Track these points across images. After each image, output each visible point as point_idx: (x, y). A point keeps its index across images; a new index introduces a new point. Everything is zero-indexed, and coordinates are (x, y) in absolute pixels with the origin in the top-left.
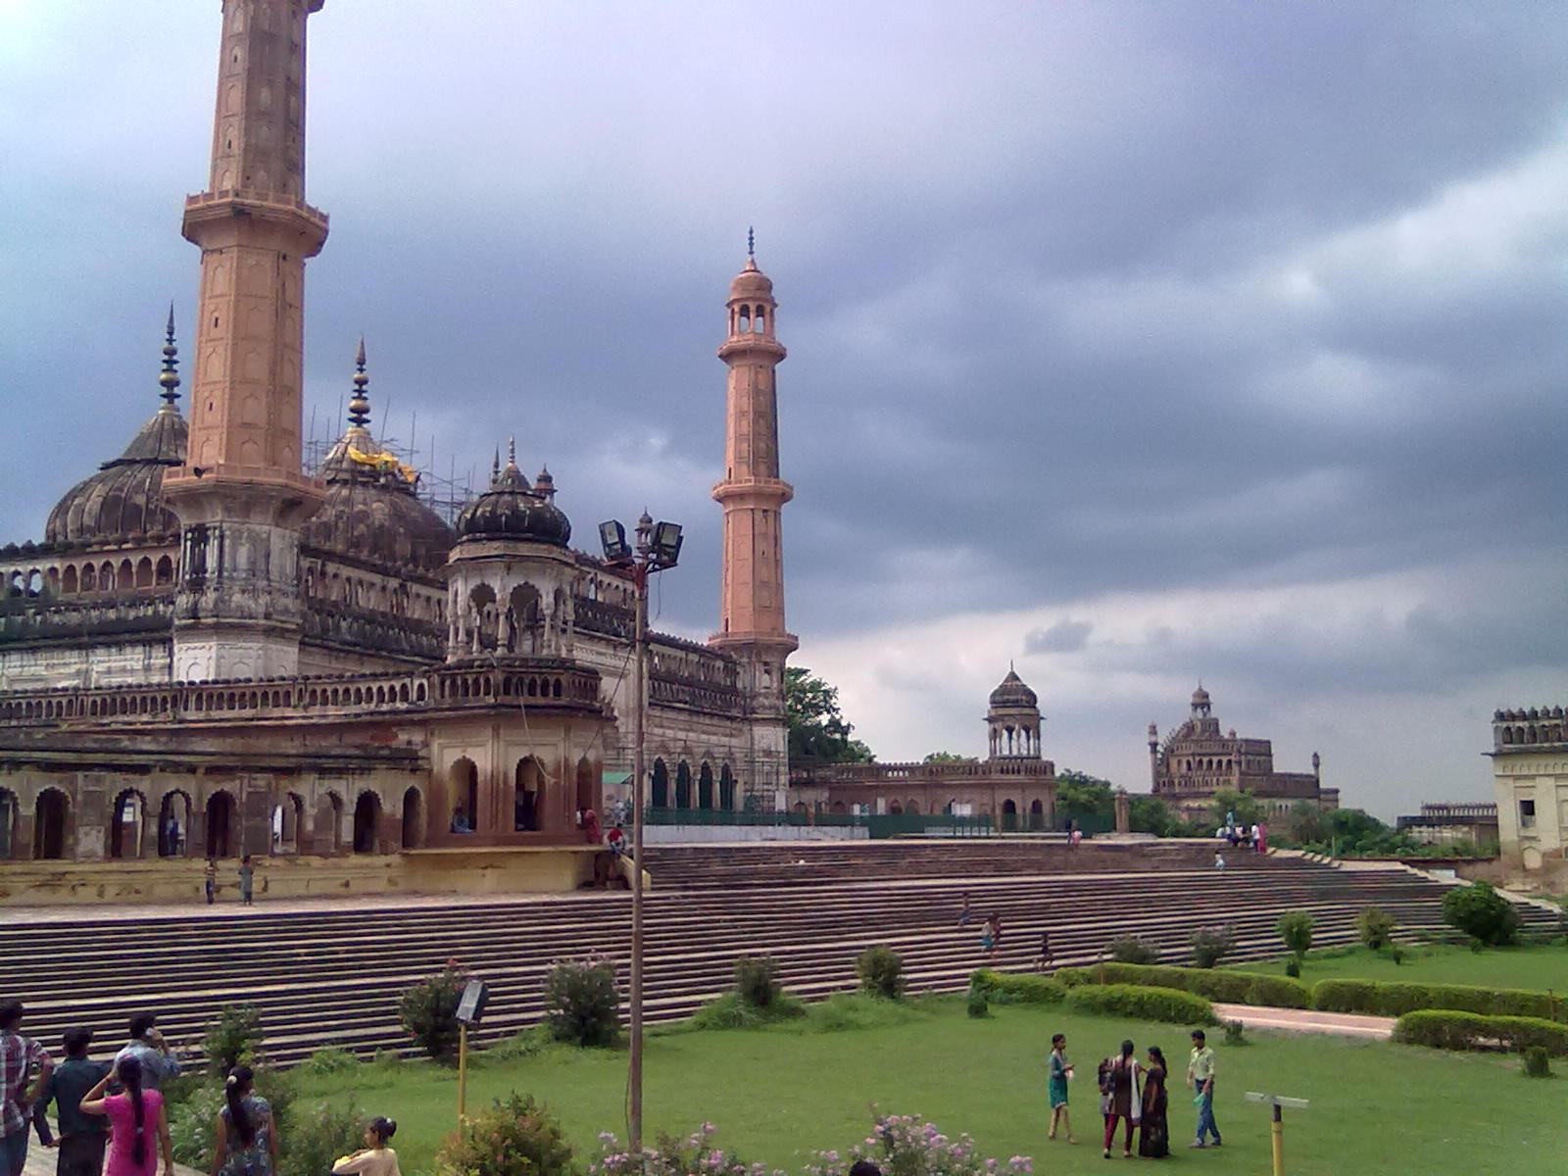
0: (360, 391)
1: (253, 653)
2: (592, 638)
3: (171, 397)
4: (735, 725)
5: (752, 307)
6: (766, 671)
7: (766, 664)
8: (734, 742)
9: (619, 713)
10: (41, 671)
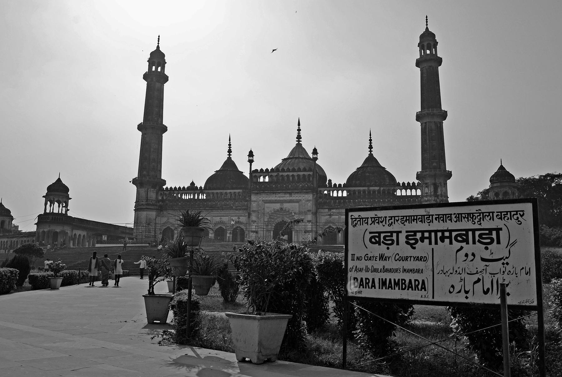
0: (299, 133)
2: (273, 193)
3: (229, 155)
9: (295, 213)
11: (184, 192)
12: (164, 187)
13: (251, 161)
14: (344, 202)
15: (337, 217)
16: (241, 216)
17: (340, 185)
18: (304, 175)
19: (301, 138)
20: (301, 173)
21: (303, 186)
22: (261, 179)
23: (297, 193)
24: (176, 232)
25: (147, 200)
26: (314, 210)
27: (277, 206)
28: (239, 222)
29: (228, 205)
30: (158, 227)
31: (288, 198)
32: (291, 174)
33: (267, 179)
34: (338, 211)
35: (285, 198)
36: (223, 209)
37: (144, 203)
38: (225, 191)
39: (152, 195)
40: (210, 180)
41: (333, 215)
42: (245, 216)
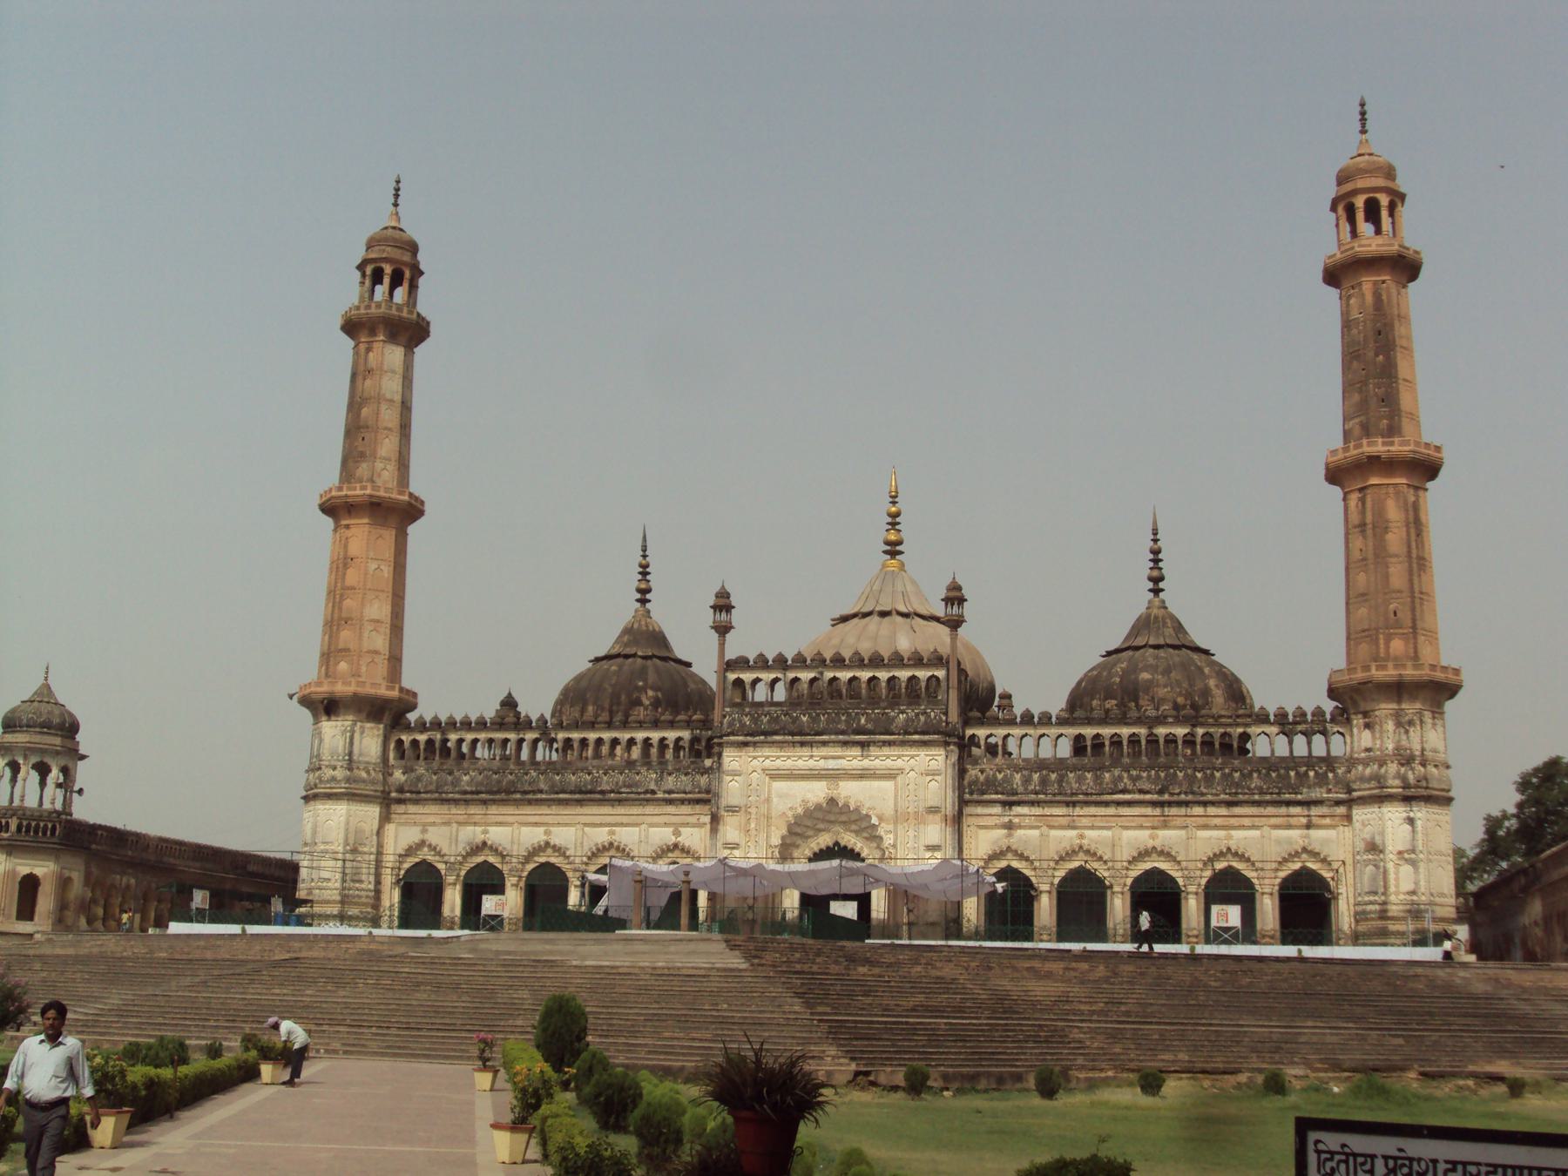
0: (893, 524)
2: (802, 744)
4: (1315, 811)
6: (1367, 726)
7: (1366, 714)
8: (1312, 832)
9: (881, 819)
11: (482, 736)
12: (412, 717)
13: (723, 630)
14: (1060, 781)
15: (1036, 833)
16: (687, 825)
17: (1046, 719)
18: (913, 677)
20: (904, 674)
21: (907, 720)
22: (761, 694)
23: (890, 744)
24: (451, 879)
25: (350, 764)
26: (950, 806)
27: (816, 792)
28: (676, 846)
29: (637, 785)
30: (389, 859)
31: (856, 763)
32: (865, 675)
33: (780, 694)
34: (1037, 811)
35: (843, 763)
36: (620, 802)
37: (339, 774)
38: (625, 736)
39: (370, 741)
40: (575, 696)
41: (1020, 827)
42: (701, 825)
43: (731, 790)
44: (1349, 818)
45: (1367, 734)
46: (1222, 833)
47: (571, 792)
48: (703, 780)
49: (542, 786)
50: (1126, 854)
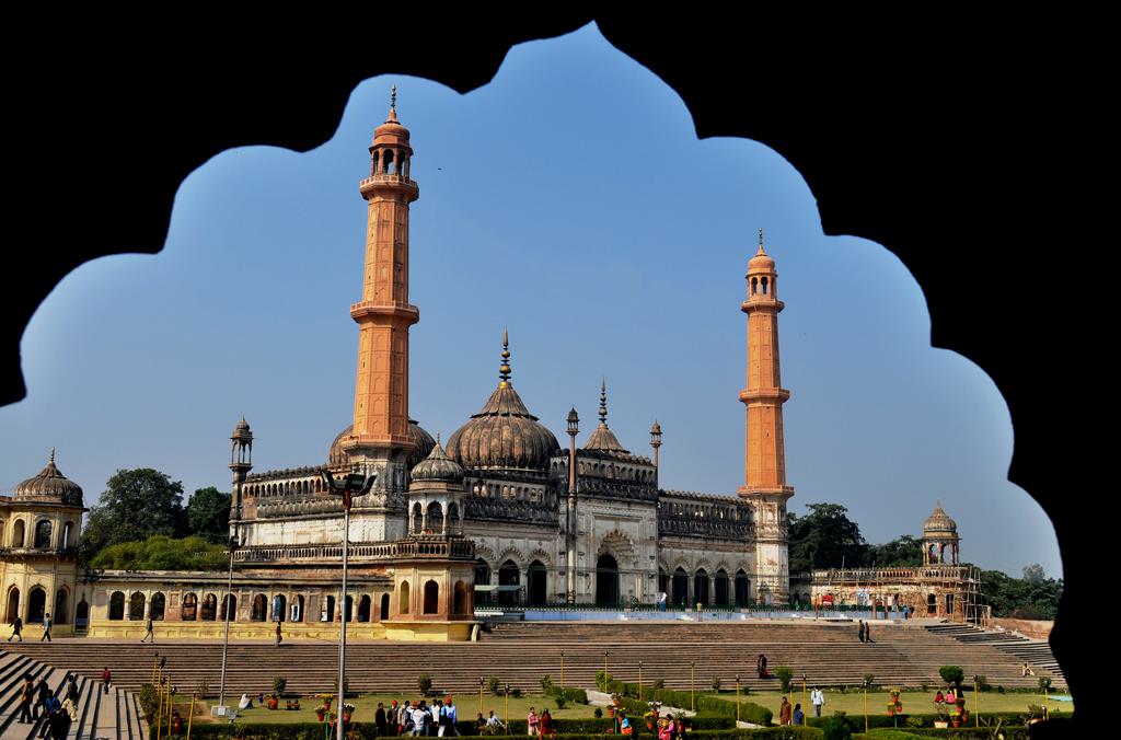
1: (379, 524)
2: (608, 501)
5: (759, 278)
10: (308, 529)
13: (573, 433)
16: (544, 539)
19: (509, 371)
20: (642, 468)
27: (610, 526)
35: (620, 512)
42: (550, 540)
43: (582, 524)
44: (754, 549)
45: (770, 514)
46: (721, 553)
47: (495, 517)
48: (552, 515)
49: (482, 513)
50: (695, 561)
